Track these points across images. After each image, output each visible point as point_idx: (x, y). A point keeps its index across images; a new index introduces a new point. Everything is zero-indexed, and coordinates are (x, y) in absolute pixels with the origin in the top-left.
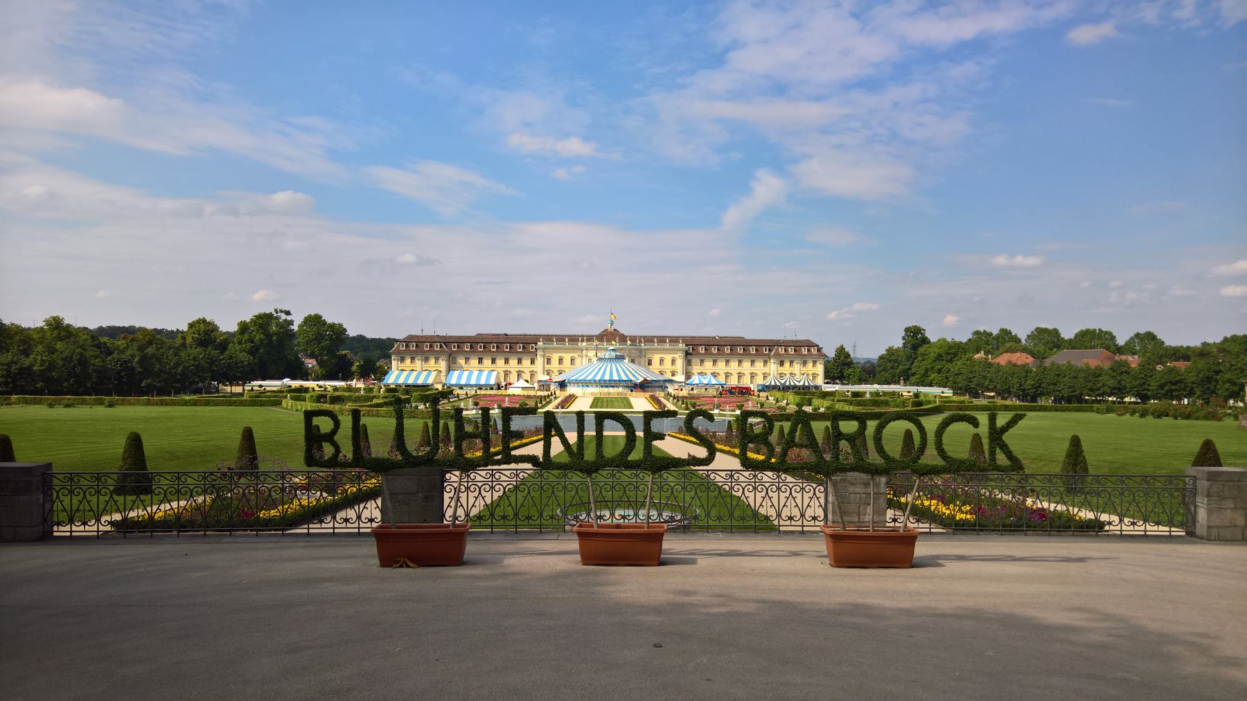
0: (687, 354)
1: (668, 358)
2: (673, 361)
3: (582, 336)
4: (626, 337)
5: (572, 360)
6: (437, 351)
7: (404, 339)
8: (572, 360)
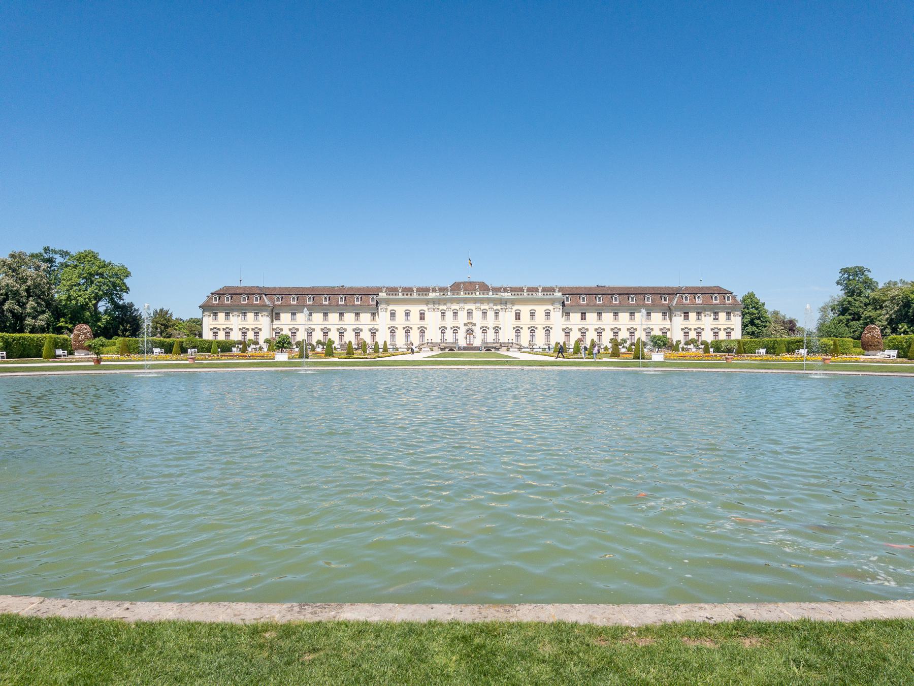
0: (564, 305)
2: (548, 314)
6: (257, 305)
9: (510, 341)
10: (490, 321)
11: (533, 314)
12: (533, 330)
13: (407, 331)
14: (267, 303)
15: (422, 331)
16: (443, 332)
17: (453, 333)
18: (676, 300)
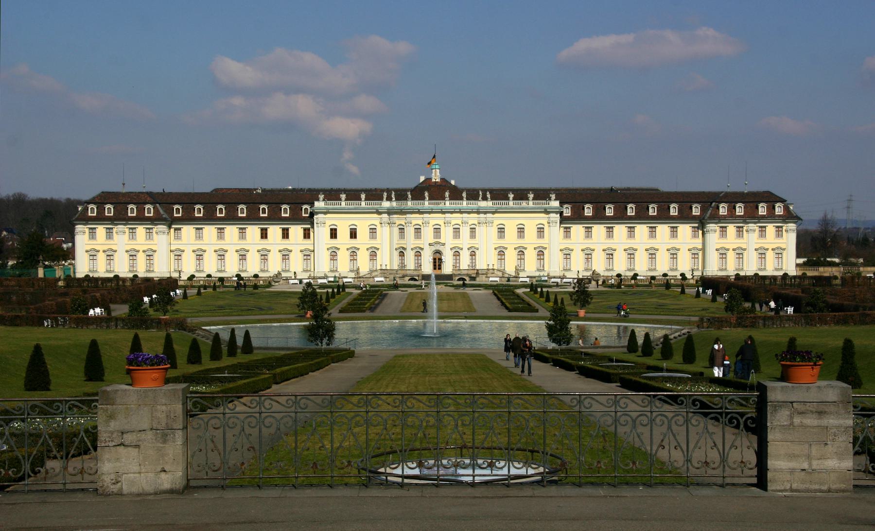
0: (563, 220)
1: (531, 222)
2: (541, 231)
3: (389, 191)
4: (461, 191)
5: (373, 231)
7: (94, 198)
8: (373, 231)
9: (491, 267)
10: (465, 241)
11: (521, 231)
12: (521, 253)
13: (354, 253)
14: (164, 216)
15: (373, 255)
16: (402, 254)
17: (415, 256)
18: (710, 211)
